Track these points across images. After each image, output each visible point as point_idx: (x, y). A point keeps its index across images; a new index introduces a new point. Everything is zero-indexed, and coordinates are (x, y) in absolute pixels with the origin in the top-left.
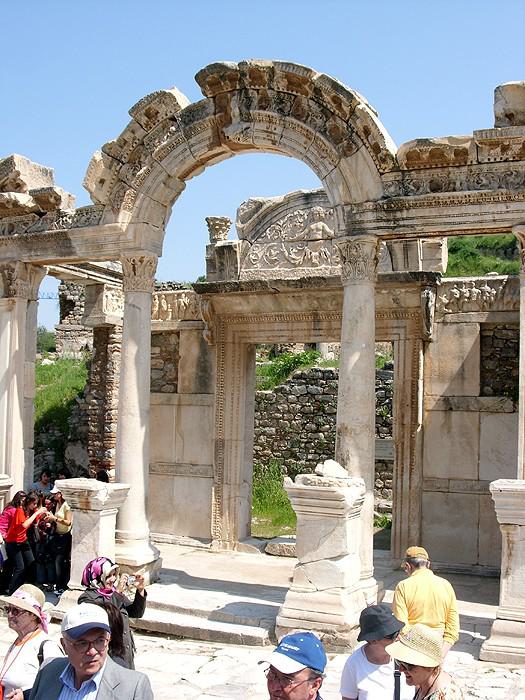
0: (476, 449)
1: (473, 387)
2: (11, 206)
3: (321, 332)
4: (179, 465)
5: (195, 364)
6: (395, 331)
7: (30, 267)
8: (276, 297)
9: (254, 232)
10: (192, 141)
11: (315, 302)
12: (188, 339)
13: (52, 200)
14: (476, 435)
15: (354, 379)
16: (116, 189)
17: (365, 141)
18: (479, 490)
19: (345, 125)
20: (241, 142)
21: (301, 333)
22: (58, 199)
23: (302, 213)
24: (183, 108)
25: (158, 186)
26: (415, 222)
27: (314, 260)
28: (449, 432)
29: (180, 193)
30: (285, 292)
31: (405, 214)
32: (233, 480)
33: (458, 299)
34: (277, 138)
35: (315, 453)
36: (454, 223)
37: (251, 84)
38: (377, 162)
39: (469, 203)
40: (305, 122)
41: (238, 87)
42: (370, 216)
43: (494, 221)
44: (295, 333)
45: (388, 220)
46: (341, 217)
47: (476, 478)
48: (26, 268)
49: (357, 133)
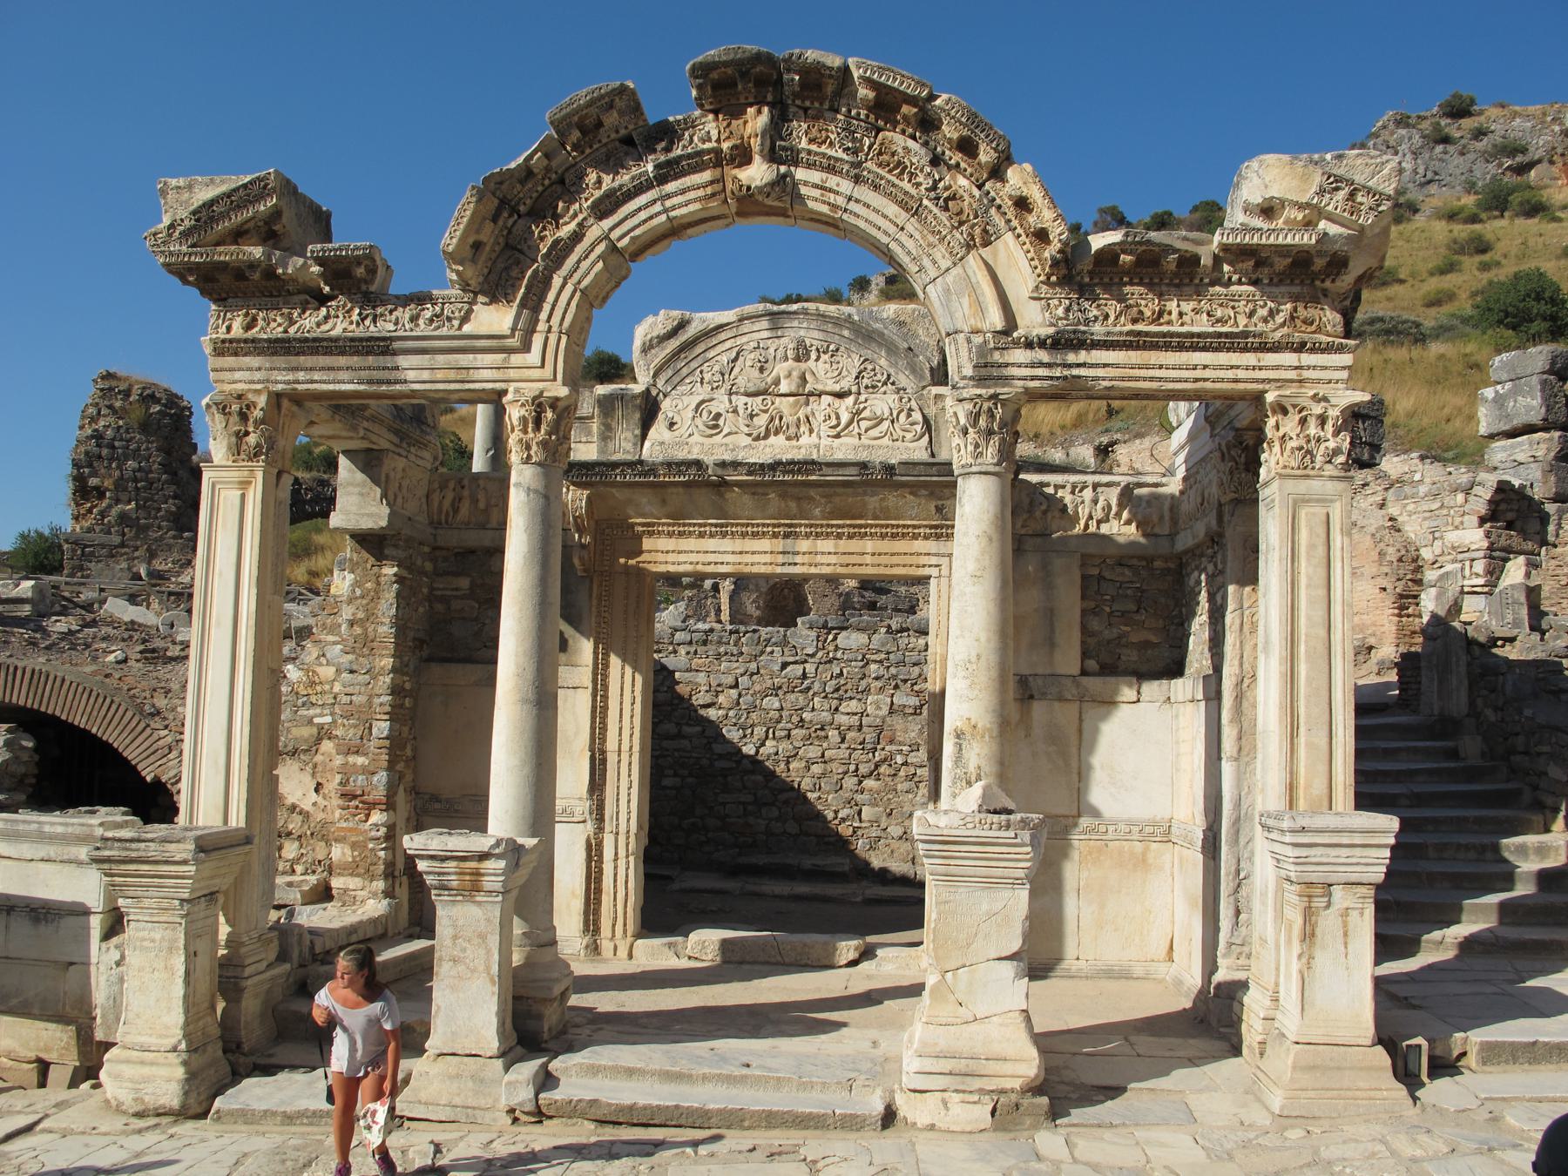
0: (1074, 764)
1: (1068, 660)
2: (257, 276)
3: (798, 559)
6: (934, 560)
7: (285, 403)
9: (670, 373)
10: (671, 187)
13: (360, 271)
14: (1074, 740)
16: (500, 265)
17: (1015, 223)
19: (976, 192)
20: (769, 202)
21: (756, 558)
22: (372, 271)
24: (651, 122)
25: (594, 264)
26: (1100, 372)
28: (1028, 735)
29: (618, 285)
30: (739, 484)
31: (1083, 356)
34: (840, 201)
35: (675, 775)
36: (1166, 380)
37: (796, 95)
38: (1036, 262)
39: (1194, 348)
40: (899, 176)
41: (770, 98)
42: (1020, 355)
43: (1236, 381)
44: (748, 558)
45: (1049, 366)
46: (964, 353)
48: (279, 406)
49: (999, 207)
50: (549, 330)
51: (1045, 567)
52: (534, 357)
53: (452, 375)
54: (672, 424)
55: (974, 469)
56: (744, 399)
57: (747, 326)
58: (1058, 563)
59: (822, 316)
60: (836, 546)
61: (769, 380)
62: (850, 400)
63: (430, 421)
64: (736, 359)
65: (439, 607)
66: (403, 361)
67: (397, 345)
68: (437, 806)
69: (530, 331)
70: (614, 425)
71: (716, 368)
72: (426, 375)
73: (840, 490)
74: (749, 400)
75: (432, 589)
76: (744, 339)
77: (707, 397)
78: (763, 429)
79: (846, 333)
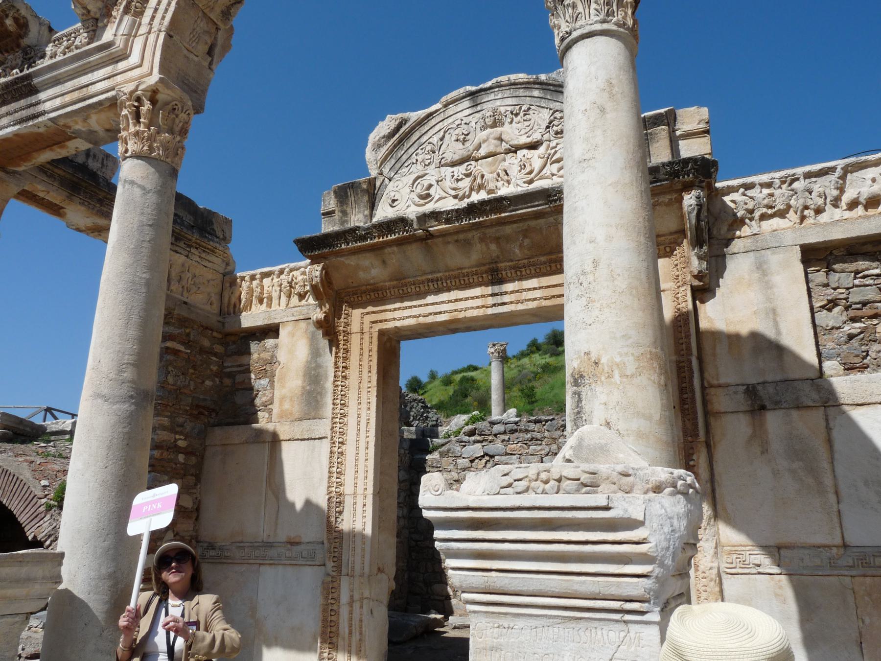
0: (828, 481)
3: (506, 298)
4: (269, 545)
5: (301, 374)
8: (427, 244)
9: (393, 161)
11: (493, 247)
12: (292, 335)
13: (9, 22)
15: (609, 238)
18: (851, 567)
23: (466, 120)
27: (491, 186)
28: (765, 451)
30: (443, 234)
32: (358, 568)
33: (751, 212)
47: (838, 541)
50: (149, 33)
51: (761, 267)
52: (134, 59)
53: (76, 95)
54: (394, 201)
55: (575, 34)
56: (450, 169)
57: (452, 109)
58: (774, 259)
59: (513, 85)
60: (539, 283)
61: (471, 148)
62: (542, 150)
63: (219, 234)
64: (442, 139)
65: (227, 381)
66: (42, 96)
67: (36, 81)
68: (212, 553)
69: (130, 36)
70: (349, 210)
71: (429, 147)
72: (58, 102)
73: (533, 223)
74: (455, 169)
75: (222, 366)
76: (450, 120)
77: (420, 173)
78: (467, 189)
79: (536, 93)
